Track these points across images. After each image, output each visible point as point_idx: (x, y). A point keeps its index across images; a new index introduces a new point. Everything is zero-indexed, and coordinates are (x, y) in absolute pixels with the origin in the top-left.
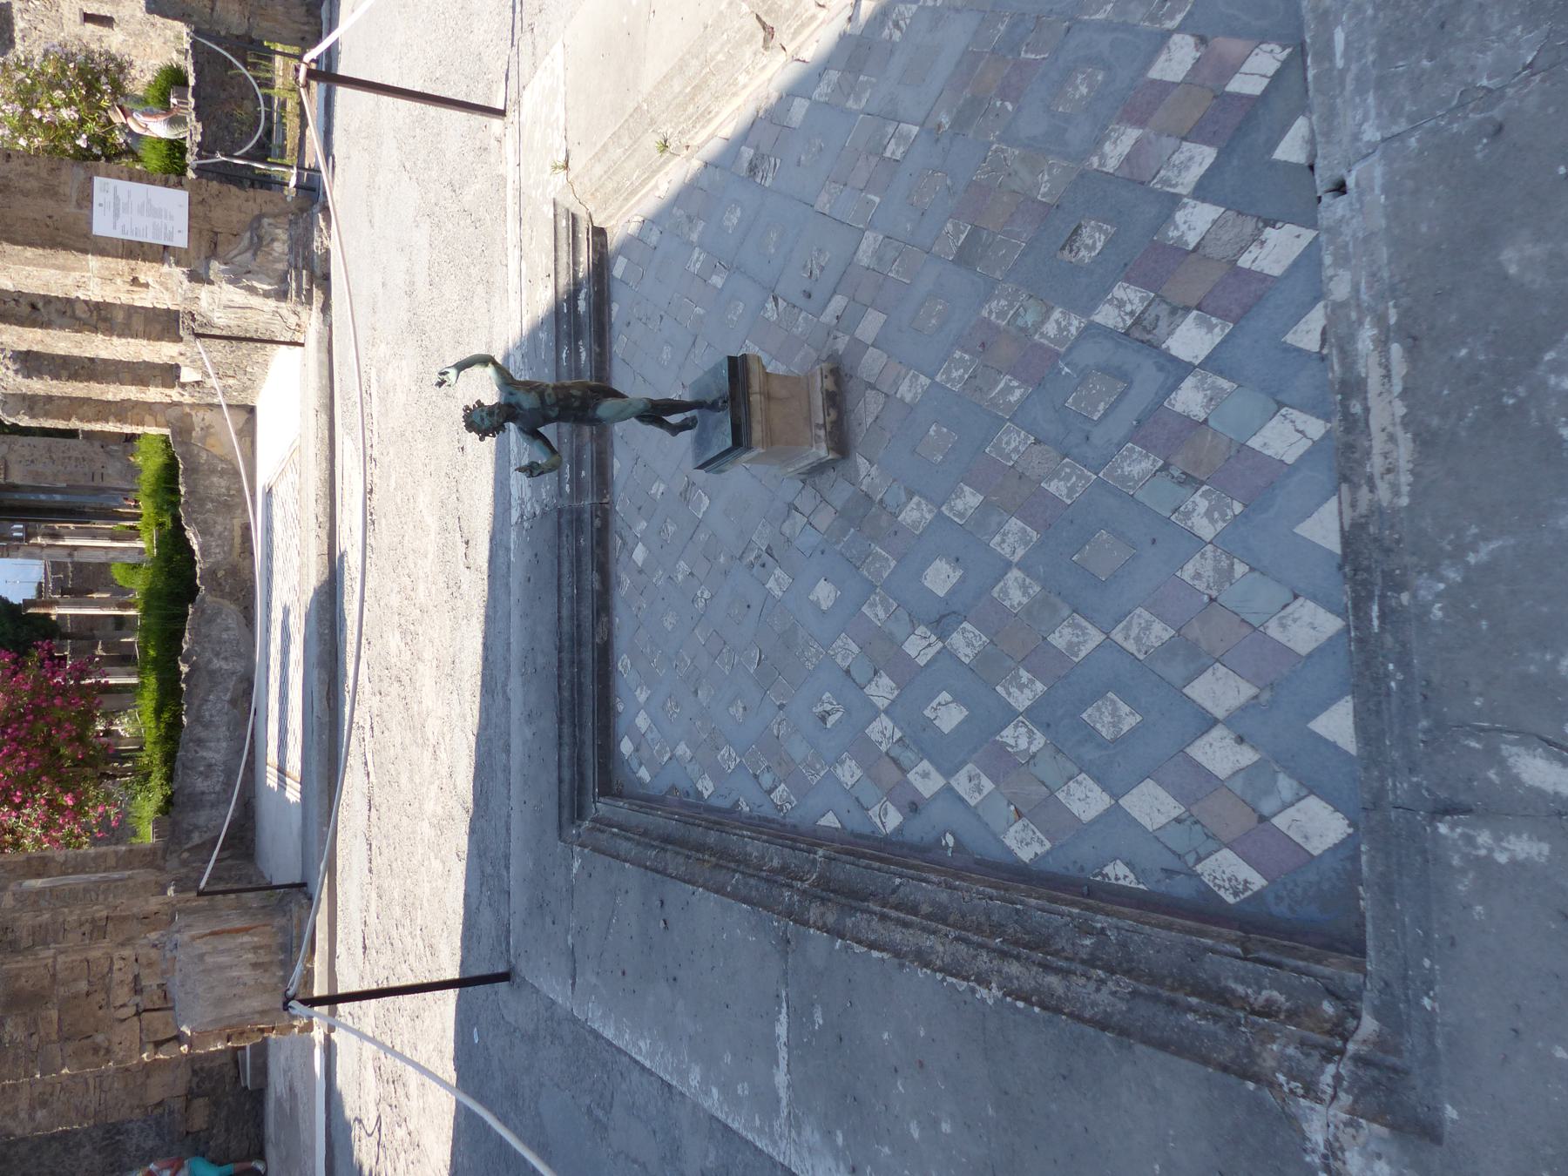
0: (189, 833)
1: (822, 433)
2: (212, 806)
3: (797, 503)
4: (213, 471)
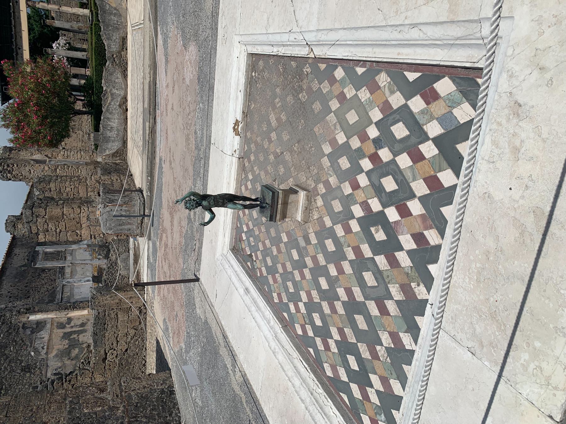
0: (105, 150)
2: (113, 142)
4: (111, 14)
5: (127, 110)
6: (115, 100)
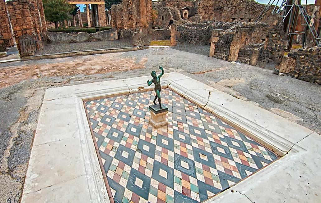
0: (50, 35)
3: (145, 122)
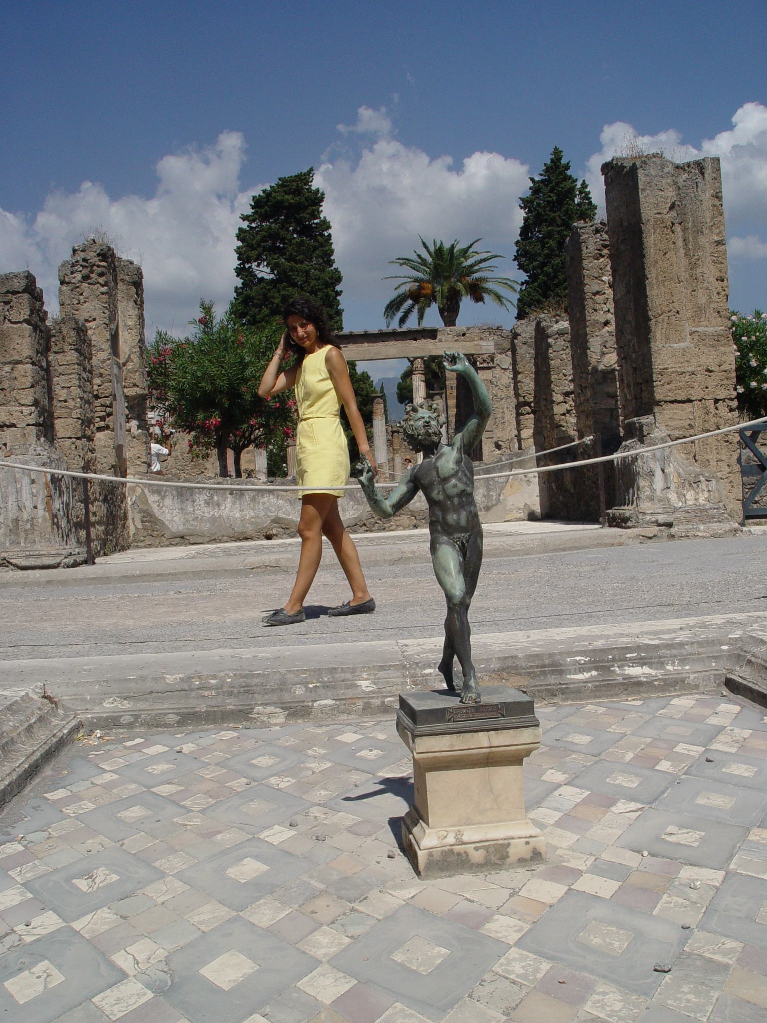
1: (451, 839)
5: (269, 538)
6: (289, 508)
